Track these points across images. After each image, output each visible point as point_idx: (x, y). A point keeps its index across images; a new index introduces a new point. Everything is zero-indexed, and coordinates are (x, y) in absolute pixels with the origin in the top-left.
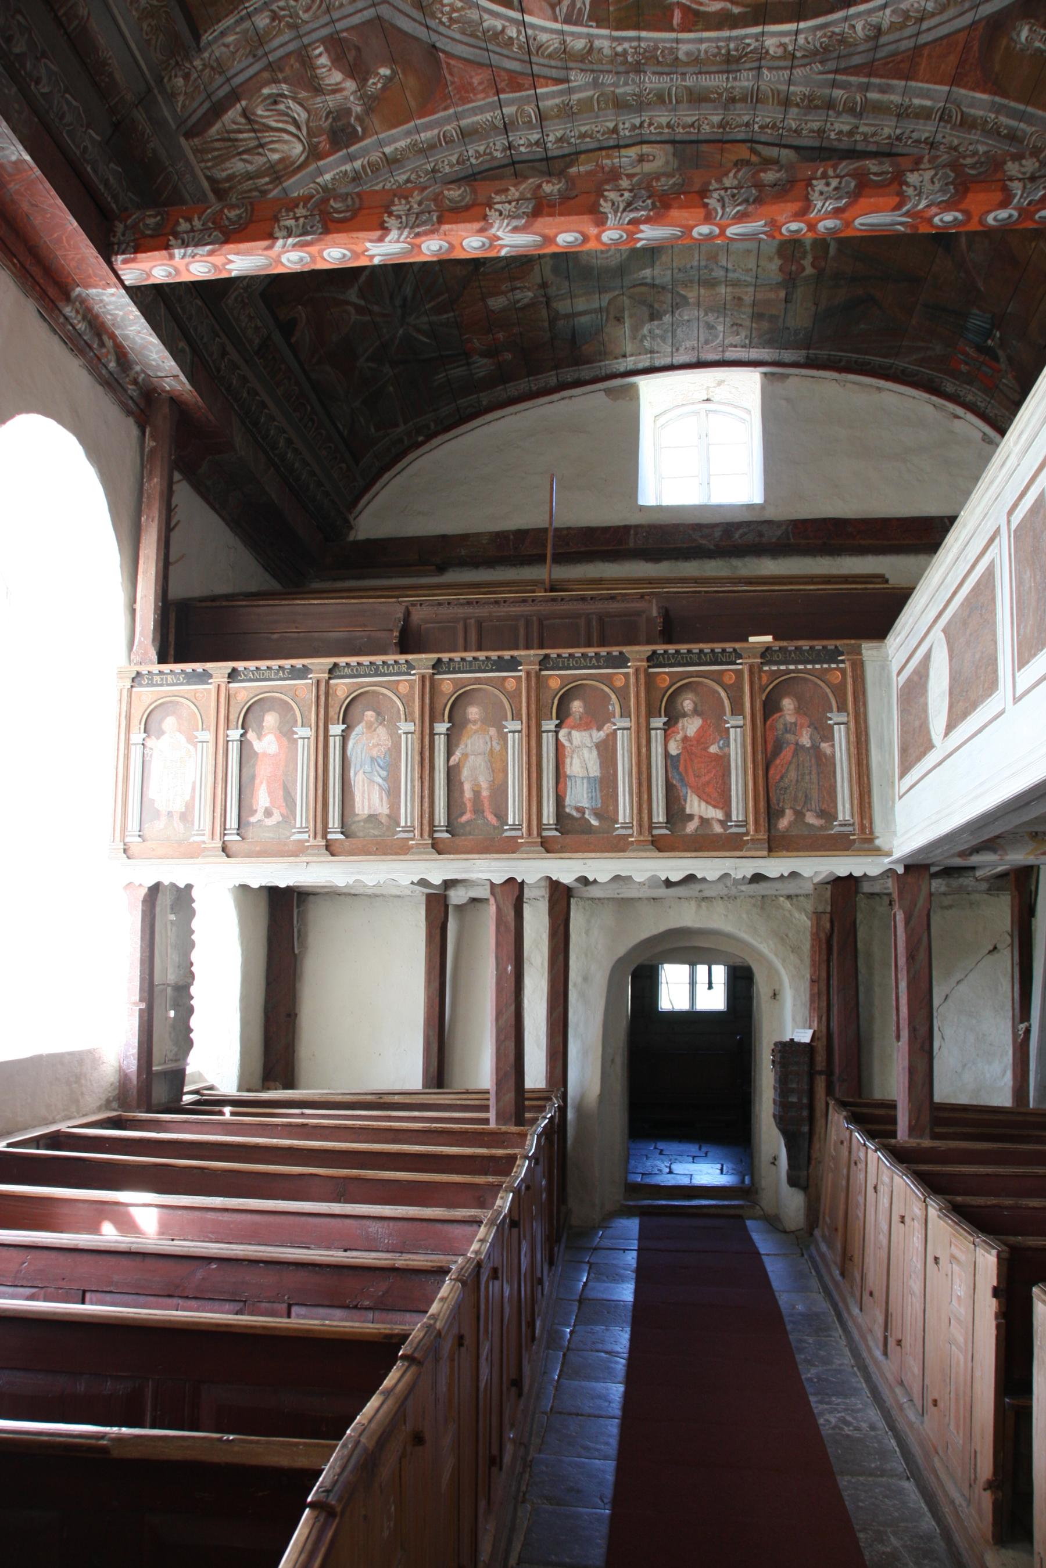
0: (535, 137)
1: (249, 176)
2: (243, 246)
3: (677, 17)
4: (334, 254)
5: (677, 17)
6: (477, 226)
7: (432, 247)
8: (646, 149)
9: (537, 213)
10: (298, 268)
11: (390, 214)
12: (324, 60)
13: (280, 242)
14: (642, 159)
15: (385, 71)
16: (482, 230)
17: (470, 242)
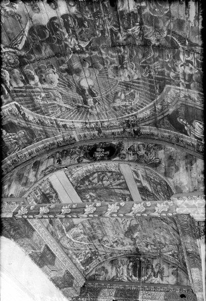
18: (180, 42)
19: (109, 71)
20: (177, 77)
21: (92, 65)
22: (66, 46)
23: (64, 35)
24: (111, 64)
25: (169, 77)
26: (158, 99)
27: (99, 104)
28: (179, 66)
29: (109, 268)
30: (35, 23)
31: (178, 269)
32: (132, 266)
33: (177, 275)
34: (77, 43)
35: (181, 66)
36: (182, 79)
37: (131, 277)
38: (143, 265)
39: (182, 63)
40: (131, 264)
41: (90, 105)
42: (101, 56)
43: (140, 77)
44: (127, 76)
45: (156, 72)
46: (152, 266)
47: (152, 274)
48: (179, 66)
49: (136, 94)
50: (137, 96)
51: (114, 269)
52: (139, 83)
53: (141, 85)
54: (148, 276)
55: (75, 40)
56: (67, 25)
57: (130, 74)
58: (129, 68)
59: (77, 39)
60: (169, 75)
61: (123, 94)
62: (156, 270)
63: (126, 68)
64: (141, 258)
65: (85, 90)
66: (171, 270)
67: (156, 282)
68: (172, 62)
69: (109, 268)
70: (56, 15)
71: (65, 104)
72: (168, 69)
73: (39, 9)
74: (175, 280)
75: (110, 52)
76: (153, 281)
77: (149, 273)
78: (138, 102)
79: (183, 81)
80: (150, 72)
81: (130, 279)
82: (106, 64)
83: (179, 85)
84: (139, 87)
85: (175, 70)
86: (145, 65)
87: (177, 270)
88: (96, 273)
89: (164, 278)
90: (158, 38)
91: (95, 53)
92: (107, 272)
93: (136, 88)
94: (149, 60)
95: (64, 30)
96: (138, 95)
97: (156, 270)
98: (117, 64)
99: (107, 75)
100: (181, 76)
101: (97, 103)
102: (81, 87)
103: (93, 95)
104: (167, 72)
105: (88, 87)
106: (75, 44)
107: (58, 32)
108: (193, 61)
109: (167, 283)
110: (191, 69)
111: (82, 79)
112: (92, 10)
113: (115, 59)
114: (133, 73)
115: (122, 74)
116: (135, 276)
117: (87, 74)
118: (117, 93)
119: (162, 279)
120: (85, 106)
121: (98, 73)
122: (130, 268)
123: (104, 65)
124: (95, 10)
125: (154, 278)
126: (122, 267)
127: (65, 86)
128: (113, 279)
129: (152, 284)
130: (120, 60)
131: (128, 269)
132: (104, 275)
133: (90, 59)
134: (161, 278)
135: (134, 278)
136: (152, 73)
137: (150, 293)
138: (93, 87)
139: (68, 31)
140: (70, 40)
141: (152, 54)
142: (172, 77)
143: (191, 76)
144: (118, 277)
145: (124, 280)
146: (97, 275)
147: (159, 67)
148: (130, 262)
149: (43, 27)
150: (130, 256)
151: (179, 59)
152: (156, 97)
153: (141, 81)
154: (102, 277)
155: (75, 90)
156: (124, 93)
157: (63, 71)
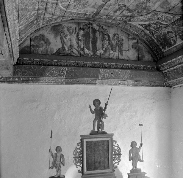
29: (50, 36)
31: (139, 41)
32: (83, 36)
33: (138, 50)
37: (83, 50)
38: (98, 35)
40: (81, 32)
46: (109, 36)
47: (110, 47)
51: (59, 38)
54: (104, 49)
62: (114, 42)
64: (95, 26)
66: (131, 42)
67: (115, 57)
69: (50, 36)
74: (136, 55)
76: (111, 56)
77: (105, 46)
81: (82, 53)
87: (138, 42)
88: (32, 43)
89: (124, 52)
92: (47, 42)
97: (114, 42)
109: (128, 59)
116: (89, 49)
119: (121, 52)
122: (80, 38)
125: (111, 52)
126: (69, 36)
128: (58, 53)
129: (110, 59)
131: (78, 39)
132: (44, 47)
134: (120, 52)
135: (87, 51)
137: (112, 71)
144: (65, 50)
145: (73, 54)
146: (33, 46)
148: (80, 29)
150: (80, 21)
154: (41, 49)
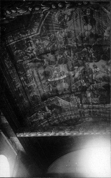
0: (74, 116)
1: (36, 121)
2: (33, 133)
3: (91, 104)
4: (45, 134)
5: (91, 104)
6: (63, 132)
7: (57, 134)
8: (89, 118)
9: (71, 131)
10: (40, 136)
11: (52, 130)
12: (47, 108)
13: (38, 133)
14: (88, 119)
15: (55, 109)
16: (64, 132)
17: (62, 134)
18: (37, 60)
19: (73, 36)
20: (34, 42)
21: (83, 39)
22: (94, 50)
23: (94, 55)
24: (72, 39)
25: (38, 39)
26: (43, 22)
27: (83, 11)
28: (35, 48)
30: (106, 61)
34: (88, 50)
35: (34, 49)
36: (32, 42)
39: (34, 50)
41: (89, 9)
42: (77, 44)
43: (55, 33)
44: (63, 33)
45: (47, 39)
48: (35, 48)
49: (57, 21)
50: (57, 19)
52: (56, 29)
53: (54, 28)
55: (89, 52)
56: (91, 58)
57: (61, 34)
58: (62, 38)
59: (88, 52)
60: (39, 41)
61: (66, 19)
63: (63, 38)
65: (90, 22)
68: (39, 48)
70: (95, 63)
71: (107, 13)
72: (40, 44)
73: (102, 66)
75: (72, 46)
78: (55, 14)
79: (31, 41)
80: (50, 38)
82: (75, 39)
83: (32, 37)
84: (56, 26)
85: (37, 45)
86: (53, 41)
90: (48, 57)
91: (80, 45)
93: (57, 25)
94: (51, 45)
95: (93, 56)
96: (56, 20)
98: (69, 39)
99: (75, 32)
100: (32, 43)
101: (84, 10)
102: (92, 25)
103: (86, 18)
104: (41, 42)
105: (88, 24)
106: (90, 50)
107: (96, 56)
108: (29, 54)
110: (29, 50)
111: (90, 30)
112: (78, 63)
113: (70, 42)
114: (59, 35)
115: (66, 34)
117: (86, 33)
118: (70, 20)
120: (93, 9)
121: (80, 34)
123: (76, 39)
124: (77, 63)
127: (102, 26)
130: (67, 42)
133: (83, 42)
136: (49, 38)
138: (85, 24)
139: (92, 56)
140: (92, 52)
141: (50, 48)
142: (36, 40)
143: (28, 46)
147: (45, 43)
149: (103, 59)
151: (36, 51)
152: (44, 22)
153: (55, 30)
155: (97, 23)
156: (65, 20)
157: (100, 37)
